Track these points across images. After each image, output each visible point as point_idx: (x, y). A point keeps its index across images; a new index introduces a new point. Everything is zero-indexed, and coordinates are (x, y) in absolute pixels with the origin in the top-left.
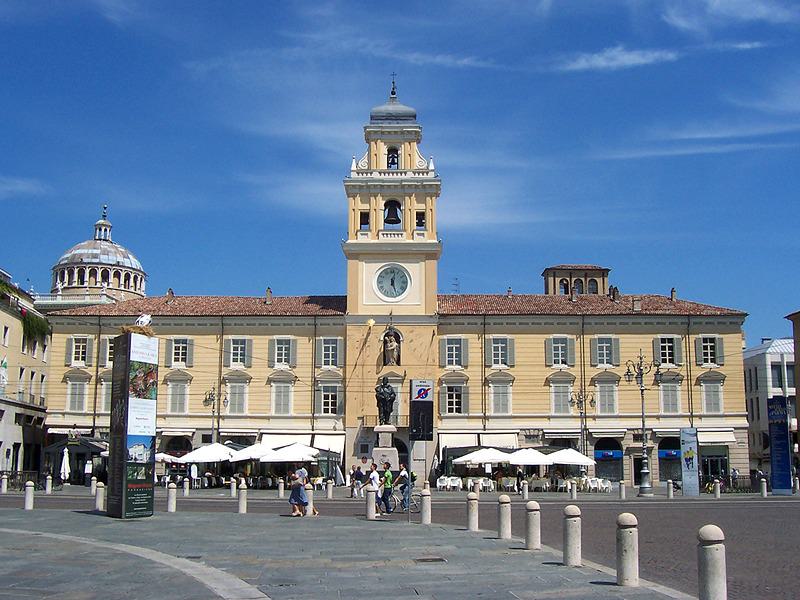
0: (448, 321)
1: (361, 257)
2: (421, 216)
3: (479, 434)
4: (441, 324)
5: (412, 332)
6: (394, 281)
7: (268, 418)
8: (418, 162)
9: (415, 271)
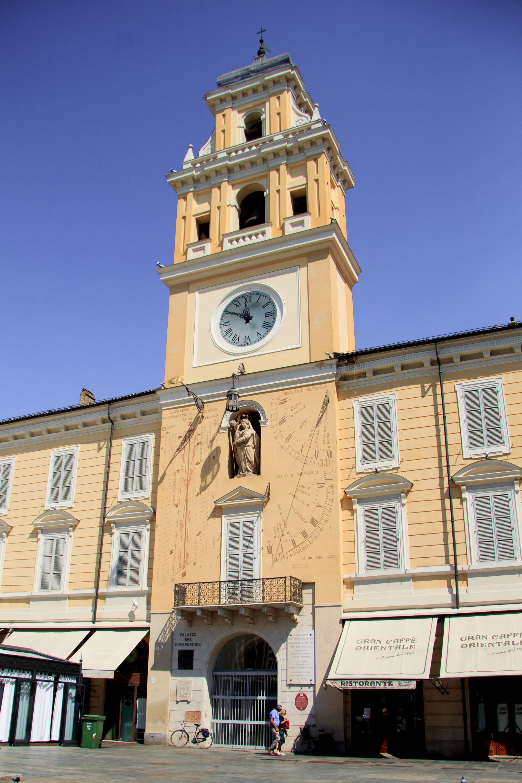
0: (356, 369)
1: (192, 286)
2: (300, 204)
3: (441, 618)
4: (344, 378)
5: (284, 402)
6: (251, 312)
7: (27, 600)
8: (294, 119)
9: (286, 287)
